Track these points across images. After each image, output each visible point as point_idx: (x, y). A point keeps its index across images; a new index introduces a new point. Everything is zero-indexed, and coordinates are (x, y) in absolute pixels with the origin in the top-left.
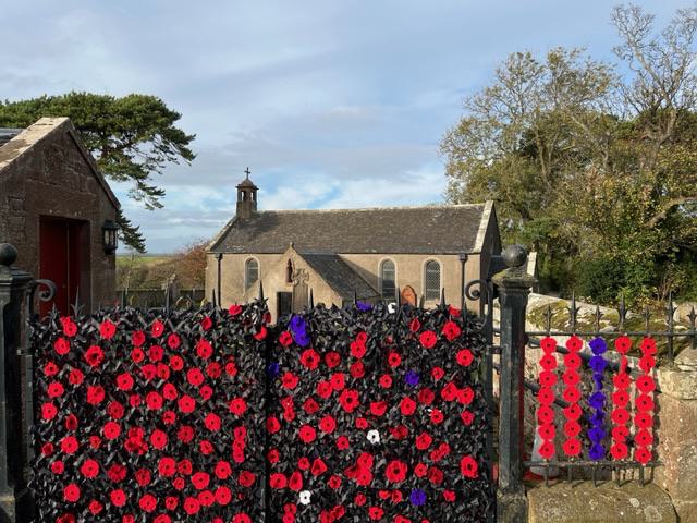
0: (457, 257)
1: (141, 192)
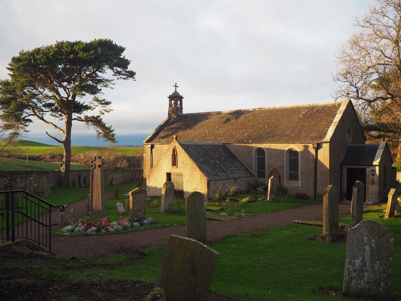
1: (96, 103)
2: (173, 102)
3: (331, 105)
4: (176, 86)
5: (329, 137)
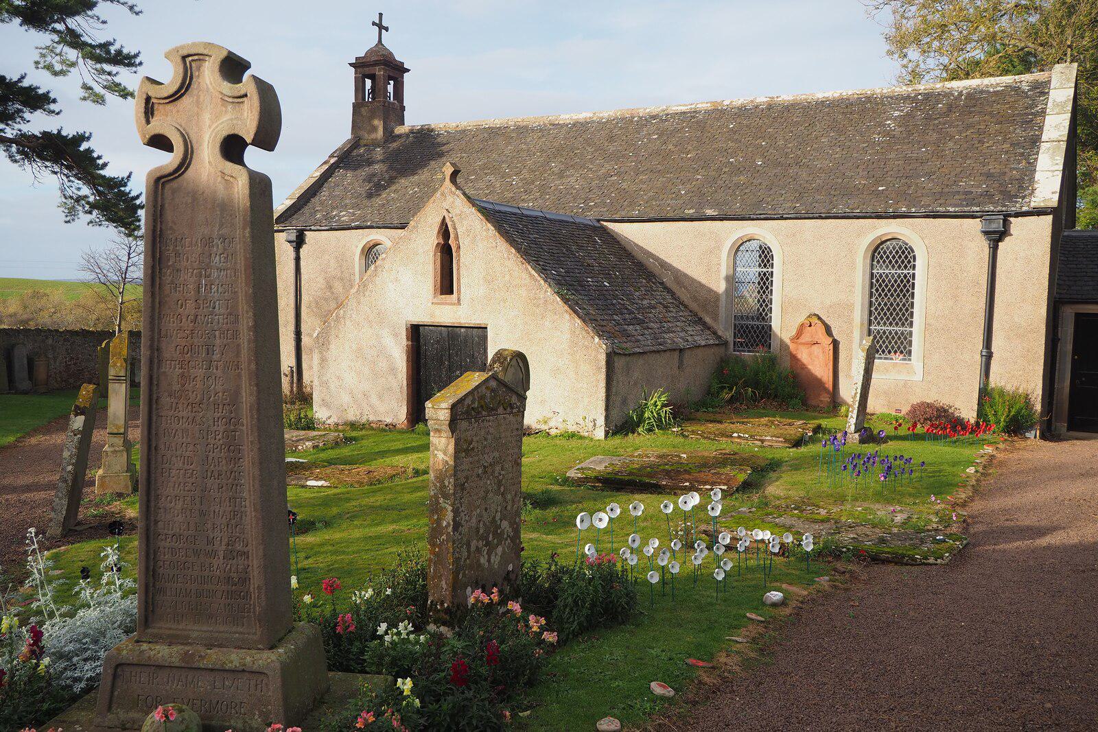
0: (975, 225)
2: (368, 83)
3: (999, 89)
4: (381, 27)
5: (1053, 193)
